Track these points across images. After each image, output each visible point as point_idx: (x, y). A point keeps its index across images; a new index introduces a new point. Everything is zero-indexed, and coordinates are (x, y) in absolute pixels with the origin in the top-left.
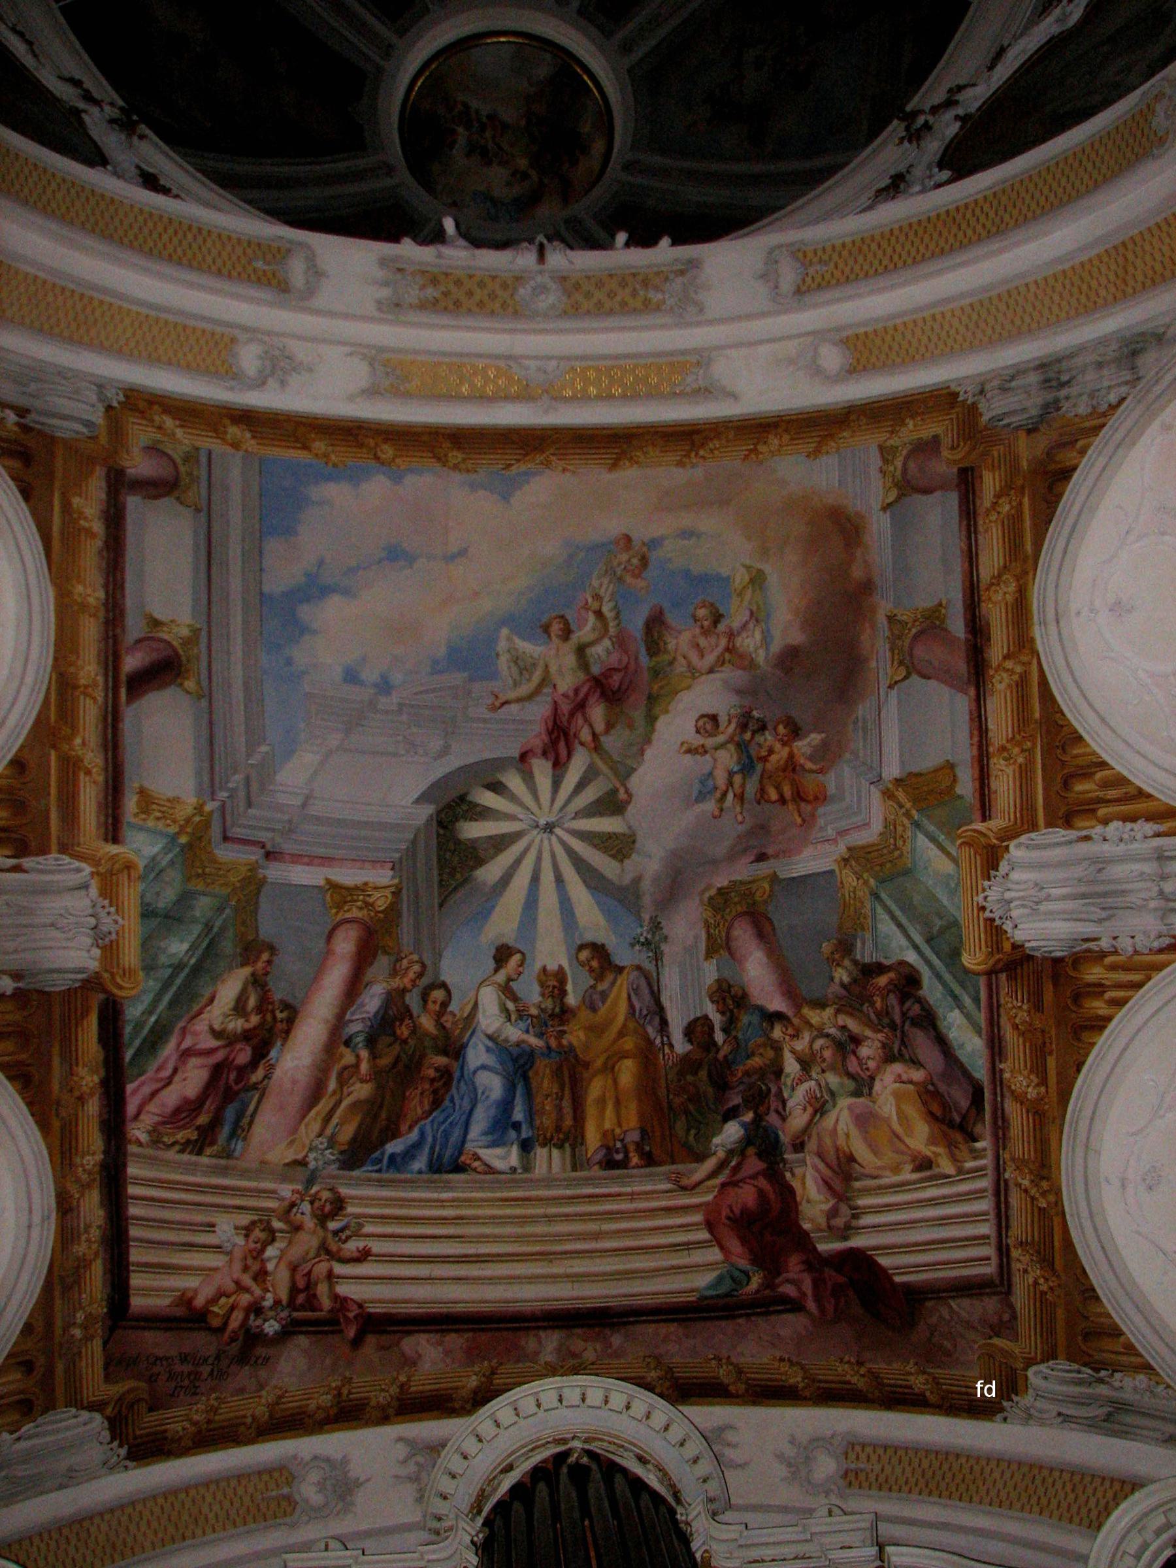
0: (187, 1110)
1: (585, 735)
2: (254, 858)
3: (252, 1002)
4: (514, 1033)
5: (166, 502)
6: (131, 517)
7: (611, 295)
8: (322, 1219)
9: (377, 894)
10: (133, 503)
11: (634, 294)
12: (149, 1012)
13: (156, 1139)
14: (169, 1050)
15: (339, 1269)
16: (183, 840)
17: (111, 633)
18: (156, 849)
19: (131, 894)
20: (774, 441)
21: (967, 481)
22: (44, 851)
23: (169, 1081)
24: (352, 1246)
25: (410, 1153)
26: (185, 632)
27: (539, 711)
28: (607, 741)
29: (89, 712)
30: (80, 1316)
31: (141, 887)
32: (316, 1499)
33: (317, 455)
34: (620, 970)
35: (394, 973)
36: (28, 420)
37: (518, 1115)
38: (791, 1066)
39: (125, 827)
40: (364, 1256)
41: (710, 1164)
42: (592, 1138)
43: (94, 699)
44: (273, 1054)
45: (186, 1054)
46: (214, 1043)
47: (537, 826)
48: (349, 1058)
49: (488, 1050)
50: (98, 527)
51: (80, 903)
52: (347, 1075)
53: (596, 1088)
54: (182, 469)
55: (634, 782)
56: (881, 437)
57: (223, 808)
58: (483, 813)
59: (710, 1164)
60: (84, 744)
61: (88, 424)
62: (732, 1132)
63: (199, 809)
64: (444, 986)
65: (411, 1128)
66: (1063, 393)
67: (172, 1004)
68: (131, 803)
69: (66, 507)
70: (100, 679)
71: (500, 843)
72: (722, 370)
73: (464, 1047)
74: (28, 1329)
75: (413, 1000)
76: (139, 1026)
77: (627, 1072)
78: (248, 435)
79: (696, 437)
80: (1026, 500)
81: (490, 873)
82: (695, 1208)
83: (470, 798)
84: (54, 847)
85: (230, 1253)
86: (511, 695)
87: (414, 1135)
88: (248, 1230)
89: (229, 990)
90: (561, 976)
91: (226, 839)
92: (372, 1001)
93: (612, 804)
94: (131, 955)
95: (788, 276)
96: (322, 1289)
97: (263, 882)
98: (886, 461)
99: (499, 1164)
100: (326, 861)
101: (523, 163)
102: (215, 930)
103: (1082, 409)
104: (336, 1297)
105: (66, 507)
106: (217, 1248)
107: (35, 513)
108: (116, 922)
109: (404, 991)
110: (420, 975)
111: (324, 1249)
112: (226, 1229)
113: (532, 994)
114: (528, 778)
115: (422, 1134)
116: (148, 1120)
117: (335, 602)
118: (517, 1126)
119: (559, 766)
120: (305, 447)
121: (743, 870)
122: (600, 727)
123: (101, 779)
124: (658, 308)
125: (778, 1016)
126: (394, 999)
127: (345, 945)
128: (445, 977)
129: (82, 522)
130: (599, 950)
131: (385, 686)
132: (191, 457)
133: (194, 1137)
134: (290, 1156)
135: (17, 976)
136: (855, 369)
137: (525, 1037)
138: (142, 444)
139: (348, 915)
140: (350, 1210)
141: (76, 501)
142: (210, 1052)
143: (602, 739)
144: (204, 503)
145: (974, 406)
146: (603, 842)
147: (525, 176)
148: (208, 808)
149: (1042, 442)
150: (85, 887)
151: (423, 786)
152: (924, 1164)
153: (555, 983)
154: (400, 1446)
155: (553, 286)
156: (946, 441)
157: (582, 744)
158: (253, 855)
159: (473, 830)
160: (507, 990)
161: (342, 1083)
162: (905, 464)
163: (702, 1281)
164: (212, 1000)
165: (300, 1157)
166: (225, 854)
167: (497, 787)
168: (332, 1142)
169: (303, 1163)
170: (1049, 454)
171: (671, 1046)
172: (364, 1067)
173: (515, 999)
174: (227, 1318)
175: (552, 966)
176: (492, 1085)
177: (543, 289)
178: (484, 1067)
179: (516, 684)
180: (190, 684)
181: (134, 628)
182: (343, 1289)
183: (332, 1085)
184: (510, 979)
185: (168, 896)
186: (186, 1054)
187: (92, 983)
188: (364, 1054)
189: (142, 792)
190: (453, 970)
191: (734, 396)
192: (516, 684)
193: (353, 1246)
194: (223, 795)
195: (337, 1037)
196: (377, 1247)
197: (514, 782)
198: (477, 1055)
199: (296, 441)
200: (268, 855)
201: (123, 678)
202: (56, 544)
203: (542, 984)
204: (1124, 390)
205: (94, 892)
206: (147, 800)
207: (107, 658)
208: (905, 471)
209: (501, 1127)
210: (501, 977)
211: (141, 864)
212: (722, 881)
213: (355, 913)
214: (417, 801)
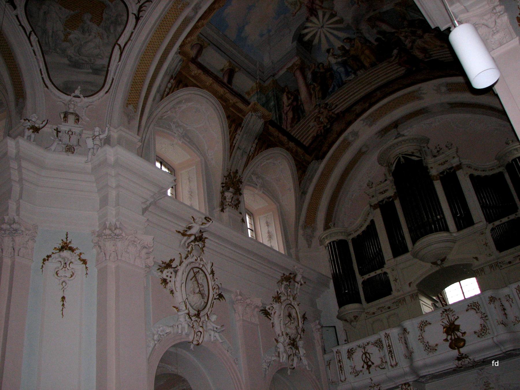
0: (293, 119)
1: (317, 7)
2: (271, 79)
3: (290, 96)
4: (340, 60)
5: (204, 51)
6: (202, 62)
8: (325, 108)
9: (297, 63)
10: (199, 60)
12: (276, 116)
13: (292, 127)
14: (284, 116)
15: (333, 111)
16: (258, 90)
17: (218, 81)
18: (256, 97)
19: (259, 107)
22: (242, 120)
23: (287, 119)
24: (333, 107)
25: (334, 89)
26: (228, 64)
27: (304, 9)
28: (324, 5)
29: (228, 96)
30: (301, 156)
31: (259, 104)
32: (353, 139)
33: (218, 8)
34: (355, 39)
35: (310, 69)
36: (174, 76)
37: (350, 70)
38: (403, 38)
39: (249, 100)
40: (336, 106)
41: (394, 58)
42: (367, 65)
43: (227, 93)
44: (299, 98)
45: (287, 113)
46: (289, 108)
47: (319, 28)
48: (312, 86)
49: (337, 65)
50: (200, 71)
51: (254, 117)
52: (314, 89)
53: (362, 57)
54: (199, 43)
55: (335, 9)
57: (260, 79)
58: (307, 34)
59: (394, 58)
60: (232, 100)
61: (180, 61)
62: (395, 52)
63: (257, 83)
64: (321, 63)
65: (331, 85)
67: (278, 110)
68: (246, 97)
69: (193, 77)
70: (224, 89)
71: (315, 35)
73: (332, 68)
74: (296, 165)
75: (317, 70)
76: (276, 118)
77: (367, 52)
78: (203, 21)
81: (316, 41)
82: (395, 64)
83: (302, 34)
84: (243, 117)
85: (315, 126)
86: (296, 11)
87: (332, 86)
88: (315, 121)
89: (285, 99)
90: (343, 47)
91: (265, 82)
92: (309, 76)
93: (333, 15)
94: (267, 113)
96: (333, 115)
97: (276, 80)
99: (351, 79)
100: (284, 66)
102: (275, 95)
104: (336, 114)
105: (193, 77)
106: (312, 127)
107: (191, 86)
108: (260, 112)
109: (314, 70)
110: (315, 65)
111: (329, 111)
112: (312, 124)
113: (339, 52)
114: (311, 22)
115: (334, 85)
116: (289, 126)
117: (246, 28)
118: (351, 72)
119: (317, 16)
120: (214, 10)
121: (372, 14)
122: (320, 4)
123: (239, 100)
125: (394, 32)
126: (314, 74)
127: (298, 74)
128: (319, 62)
129: (197, 75)
130: (347, 38)
131: (269, 31)
132: (199, 38)
133: (297, 120)
134: (314, 106)
135: (256, 138)
137: (343, 59)
138: (190, 49)
139: (295, 70)
140: (329, 103)
141: (193, 74)
142: (289, 109)
143: (323, 5)
144: (210, 43)
146: (336, 22)
148: (258, 82)
150: (252, 115)
151: (291, 39)
152: (441, 46)
153: (342, 48)
154: (361, 121)
157: (318, 9)
158: (271, 79)
159: (307, 38)
160: (333, 55)
161: (313, 90)
163: (403, 72)
164: (283, 103)
165: (315, 105)
166: (266, 84)
167: (306, 28)
168: (319, 98)
169: (316, 105)
171: (374, 44)
172: (316, 85)
173: (336, 55)
174: (321, 132)
175: (340, 46)
176: (342, 69)
178: (338, 68)
179: (295, 8)
180: (237, 69)
181: (220, 75)
182: (336, 112)
183: (312, 92)
184: (333, 53)
185: (264, 99)
186: (287, 113)
187: (265, 123)
188: (314, 84)
189: (246, 93)
190: (320, 60)
192: (295, 8)
193: (333, 107)
194: (258, 77)
195: (307, 86)
196: (338, 103)
197: (309, 24)
198: (335, 68)
199: (212, 10)
200: (274, 76)
201: (227, 84)
202: (198, 84)
203: (340, 50)
205: (254, 114)
206: (248, 93)
207: (222, 86)
209: (347, 74)
210: (331, 54)
211: (256, 101)
212: (367, 17)
213: (296, 68)
214: (292, 43)
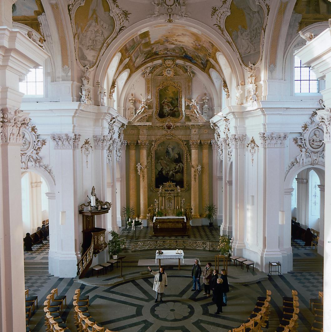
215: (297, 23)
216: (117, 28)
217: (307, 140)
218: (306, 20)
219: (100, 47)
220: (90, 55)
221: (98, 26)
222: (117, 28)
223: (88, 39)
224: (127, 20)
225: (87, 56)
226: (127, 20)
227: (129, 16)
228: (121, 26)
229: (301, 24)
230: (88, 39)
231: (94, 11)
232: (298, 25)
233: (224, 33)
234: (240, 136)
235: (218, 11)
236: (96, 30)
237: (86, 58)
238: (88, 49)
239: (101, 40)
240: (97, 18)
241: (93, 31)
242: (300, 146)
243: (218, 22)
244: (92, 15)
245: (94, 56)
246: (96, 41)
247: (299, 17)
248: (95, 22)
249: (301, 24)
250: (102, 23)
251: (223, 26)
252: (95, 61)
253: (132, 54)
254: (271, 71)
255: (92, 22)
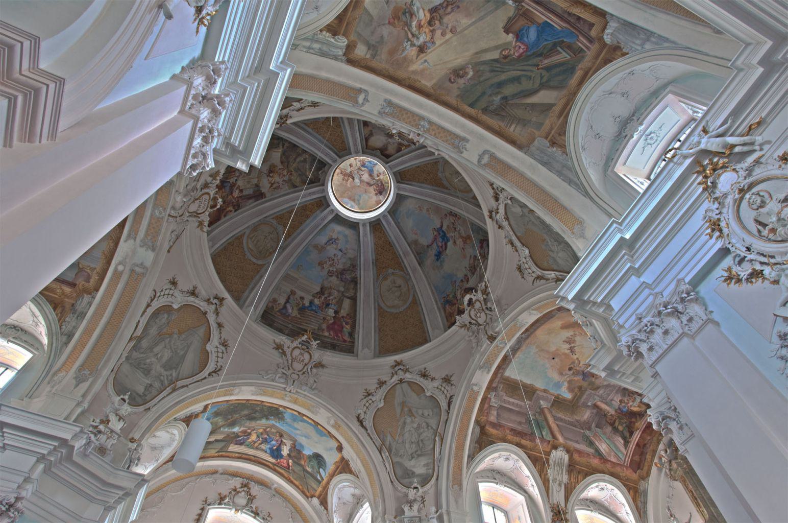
7: (154, 228)
11: (152, 233)
20: (112, 245)
21: (73, 285)
56: (98, 269)
66: (76, 316)
72: (131, 242)
79: (121, 228)
80: (57, 296)
95: (138, 270)
98: (91, 268)
101: (381, 177)
103: (67, 319)
124: (146, 237)
136: (116, 270)
145: (90, 294)
147: (378, 176)
149: (68, 306)
155: (161, 216)
156: (86, 284)
162: (87, 272)
170: (63, 307)
177: (160, 213)
191: (125, 241)
204: (63, 330)
208: (85, 272)
215: (550, 150)
216: (444, 404)
217: (749, 240)
218: (553, 132)
219: (431, 446)
220: (419, 467)
221: (416, 419)
222: (444, 404)
223: (407, 446)
224: (452, 385)
225: (414, 470)
226: (452, 385)
227: (452, 379)
228: (448, 398)
229: (554, 143)
230: (407, 446)
231: (403, 404)
232: (554, 149)
233: (547, 276)
234: (662, 409)
235: (522, 265)
236: (415, 426)
237: (413, 473)
238: (412, 458)
239: (429, 435)
240: (410, 411)
241: (412, 429)
242: (756, 274)
243: (533, 274)
244: (402, 410)
245: (426, 465)
246: (422, 440)
247: (540, 142)
248: (410, 416)
249: (554, 143)
250: (420, 412)
251: (539, 272)
252: (431, 471)
253: (554, 437)
254: (581, 237)
255: (406, 419)
